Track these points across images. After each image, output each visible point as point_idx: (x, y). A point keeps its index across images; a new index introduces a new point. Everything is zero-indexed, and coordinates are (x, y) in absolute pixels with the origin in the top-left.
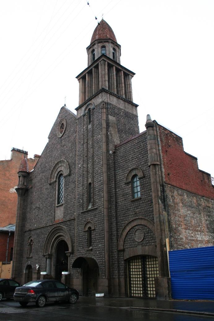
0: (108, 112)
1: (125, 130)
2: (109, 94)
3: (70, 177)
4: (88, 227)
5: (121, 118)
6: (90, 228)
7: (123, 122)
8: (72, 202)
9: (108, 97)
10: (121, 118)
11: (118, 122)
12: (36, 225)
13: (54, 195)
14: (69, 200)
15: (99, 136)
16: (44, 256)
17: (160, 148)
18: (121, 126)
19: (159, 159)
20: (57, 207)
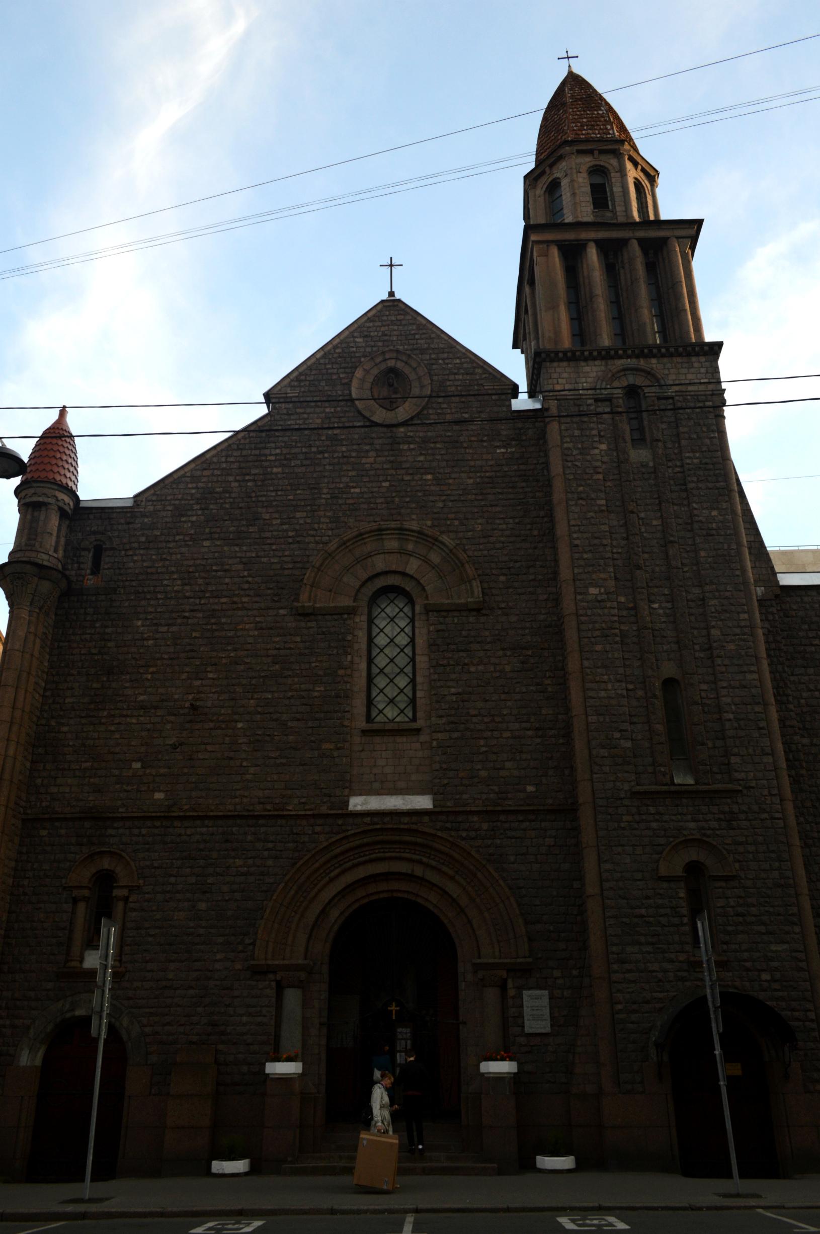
3: (482, 619)
4: (694, 858)
6: (694, 869)
8: (507, 734)
12: (159, 796)
13: (341, 672)
14: (475, 719)
15: (714, 513)
16: (259, 972)
20: (364, 732)
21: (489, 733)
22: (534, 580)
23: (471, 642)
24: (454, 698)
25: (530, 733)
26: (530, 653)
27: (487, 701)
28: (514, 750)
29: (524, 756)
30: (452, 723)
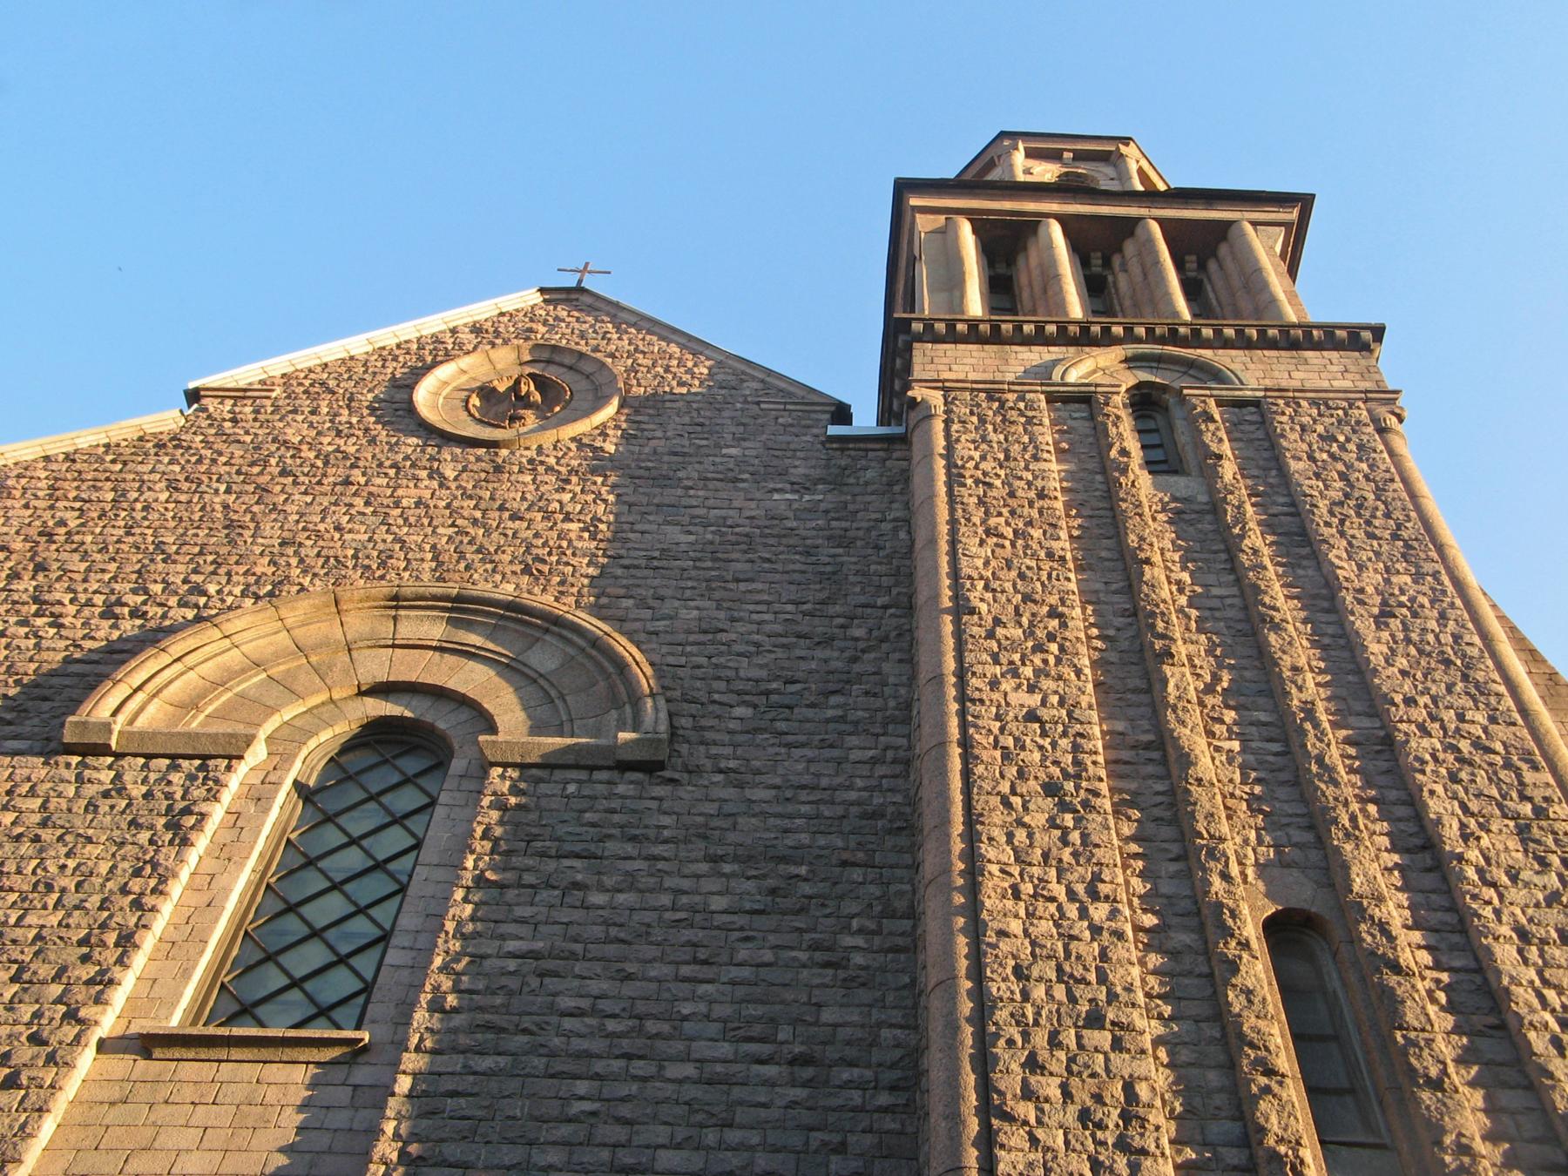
3: (659, 791)
21: (617, 1065)
22: (842, 719)
23: (610, 836)
24: (512, 965)
25: (770, 1071)
26: (803, 870)
27: (629, 977)
28: (699, 1117)
29: (733, 1136)
30: (488, 1027)
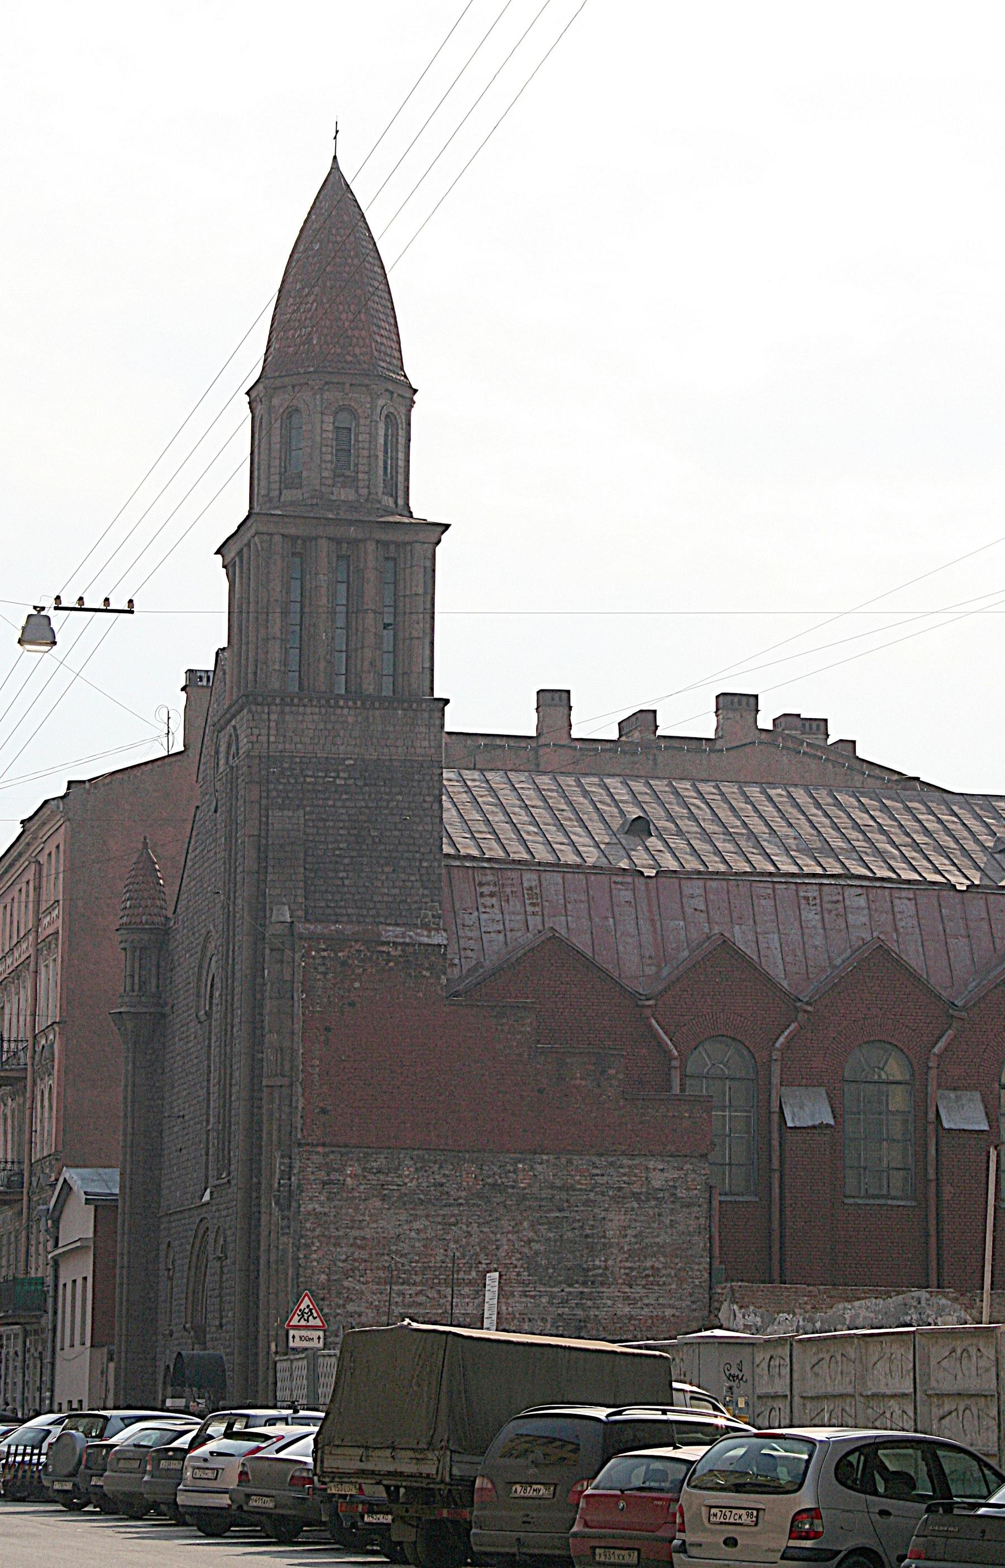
0: (267, 798)
1: (354, 854)
2: (276, 705)
5: (339, 804)
7: (345, 817)
9: (273, 724)
10: (339, 804)
11: (321, 824)
17: (298, 1026)
18: (336, 841)
19: (287, 1068)
